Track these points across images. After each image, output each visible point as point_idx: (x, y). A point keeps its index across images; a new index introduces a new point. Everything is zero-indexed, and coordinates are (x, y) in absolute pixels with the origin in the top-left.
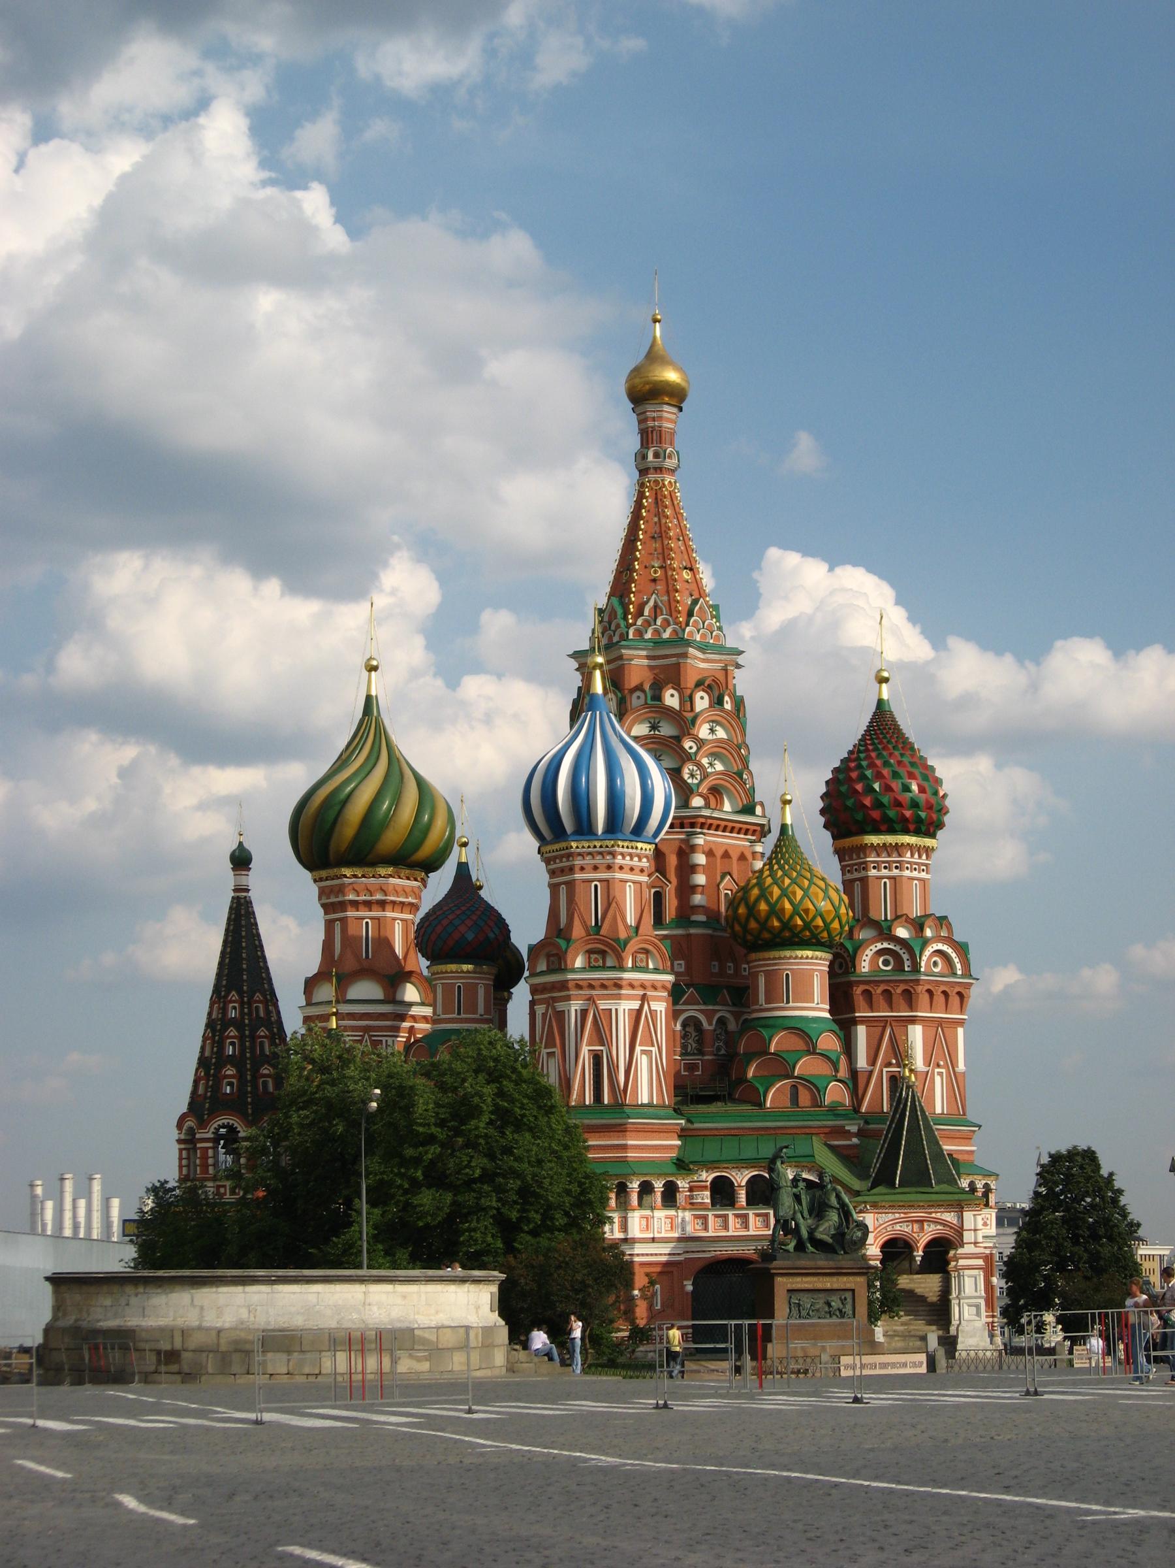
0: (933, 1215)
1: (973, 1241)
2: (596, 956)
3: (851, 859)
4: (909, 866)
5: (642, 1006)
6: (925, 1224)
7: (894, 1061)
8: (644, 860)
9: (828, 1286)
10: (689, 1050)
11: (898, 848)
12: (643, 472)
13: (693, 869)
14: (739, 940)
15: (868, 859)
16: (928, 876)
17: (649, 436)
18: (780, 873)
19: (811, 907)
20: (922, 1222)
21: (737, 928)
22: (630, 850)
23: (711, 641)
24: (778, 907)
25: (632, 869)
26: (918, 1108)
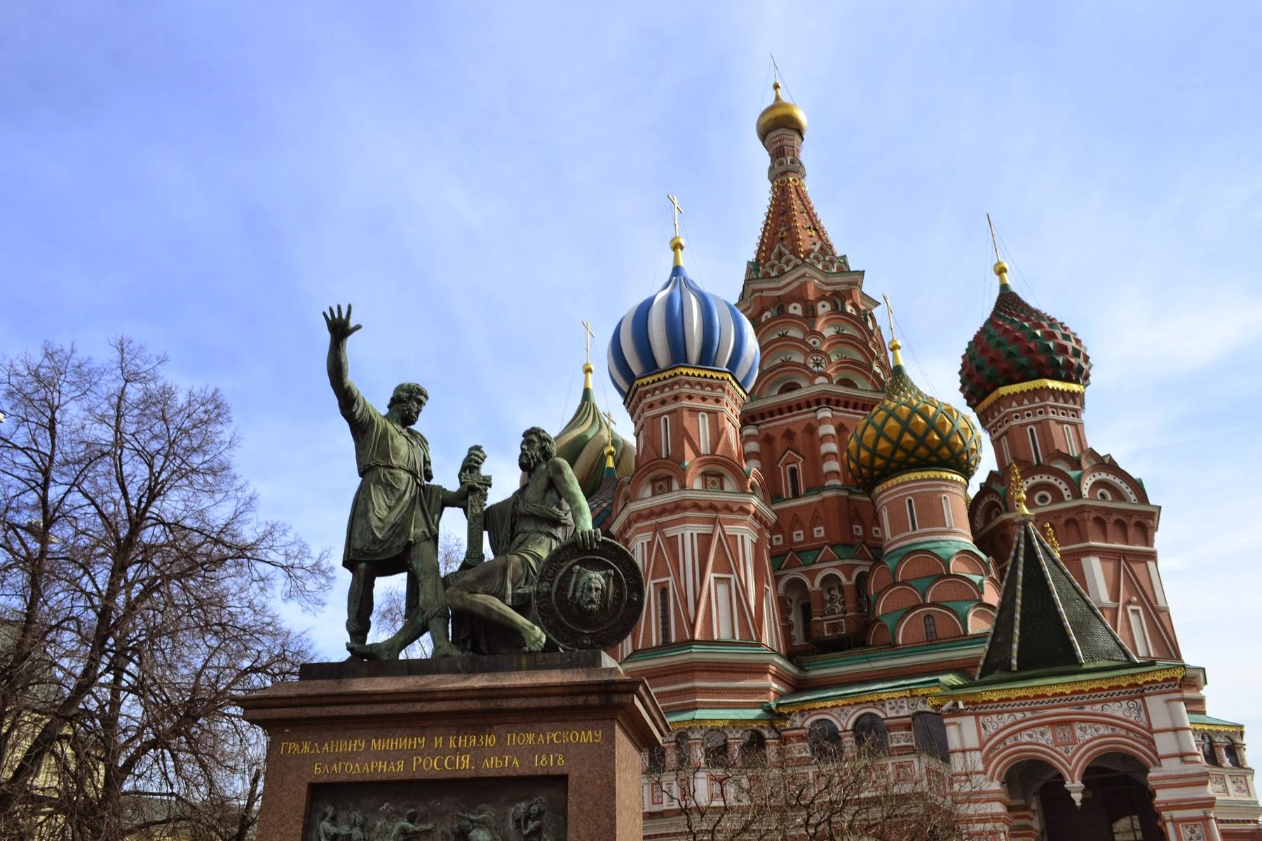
0: (1088, 709)
1: (1175, 750)
2: (661, 483)
4: (1055, 410)
6: (1077, 726)
8: (720, 390)
10: (837, 611)
11: (1036, 392)
14: (859, 481)
15: (1008, 410)
17: (778, 154)
19: (920, 420)
21: (852, 465)
22: (699, 379)
23: (834, 270)
24: (885, 428)
25: (704, 399)
26: (1039, 549)
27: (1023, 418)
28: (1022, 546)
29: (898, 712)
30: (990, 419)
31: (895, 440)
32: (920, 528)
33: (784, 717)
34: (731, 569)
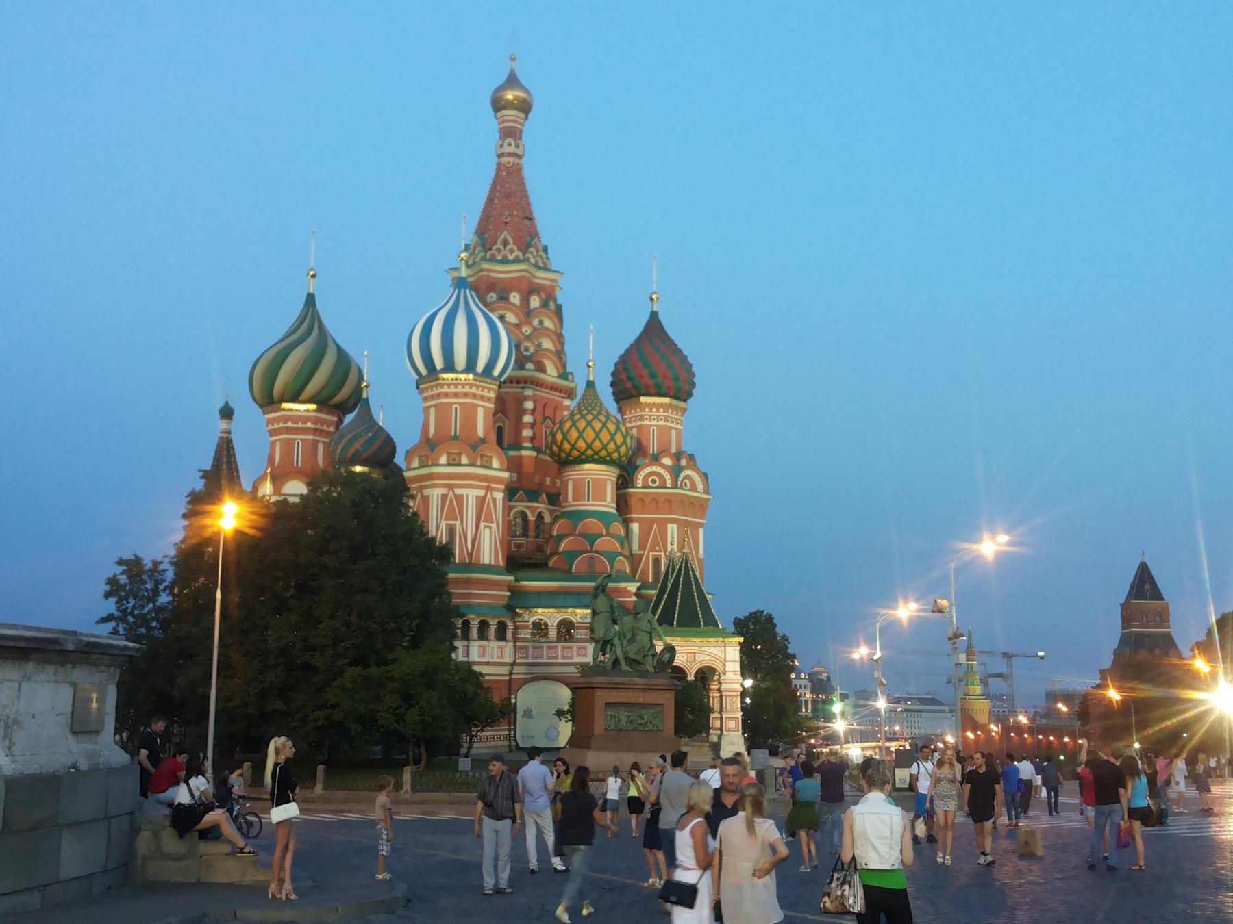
0: (703, 649)
2: (454, 456)
3: (631, 413)
5: (486, 494)
6: (697, 655)
7: (657, 548)
8: (492, 392)
9: (641, 700)
12: (500, 156)
13: (524, 412)
15: (643, 413)
16: (681, 428)
17: (510, 133)
18: (585, 412)
20: (695, 653)
21: (555, 449)
23: (542, 266)
25: (482, 398)
26: (690, 569)
27: (650, 420)
28: (683, 565)
29: (584, 620)
30: (628, 413)
31: (589, 442)
32: (593, 500)
33: (518, 615)
34: (493, 519)
